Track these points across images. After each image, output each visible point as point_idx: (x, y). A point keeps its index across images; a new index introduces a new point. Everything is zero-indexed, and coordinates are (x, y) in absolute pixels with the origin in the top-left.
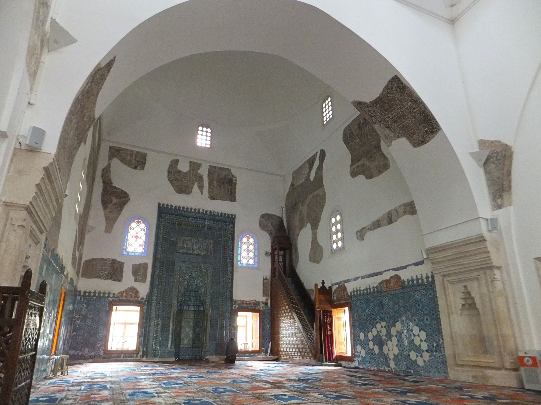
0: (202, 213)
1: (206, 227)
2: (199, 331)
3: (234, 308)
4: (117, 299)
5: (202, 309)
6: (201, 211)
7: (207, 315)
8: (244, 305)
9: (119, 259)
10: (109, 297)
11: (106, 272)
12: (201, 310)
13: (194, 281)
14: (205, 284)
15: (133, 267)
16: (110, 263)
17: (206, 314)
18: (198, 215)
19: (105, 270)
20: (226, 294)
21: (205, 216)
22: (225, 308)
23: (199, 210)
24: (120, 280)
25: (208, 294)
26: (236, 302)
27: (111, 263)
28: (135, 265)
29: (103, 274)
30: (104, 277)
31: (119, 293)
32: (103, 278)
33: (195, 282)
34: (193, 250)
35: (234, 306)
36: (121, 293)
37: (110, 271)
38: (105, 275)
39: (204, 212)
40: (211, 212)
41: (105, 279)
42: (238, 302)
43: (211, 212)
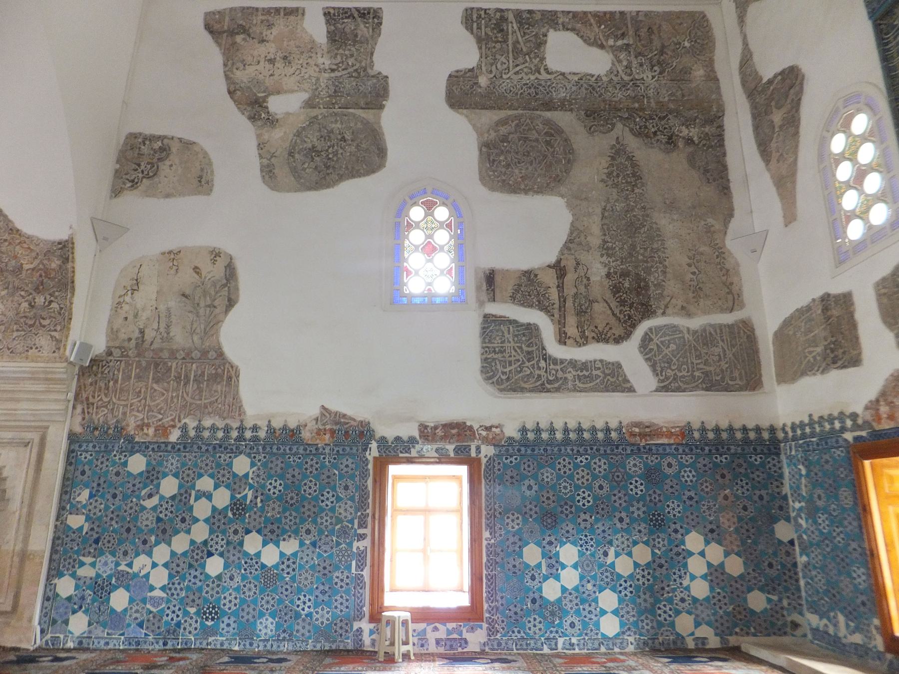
4: (864, 434)
9: (836, 288)
10: (843, 429)
11: (817, 346)
15: (879, 296)
16: (819, 312)
19: (814, 342)
24: (855, 361)
27: (823, 310)
28: (884, 279)
29: (814, 357)
30: (819, 367)
31: (867, 408)
32: (818, 370)
36: (873, 406)
37: (825, 339)
38: (818, 358)
41: (823, 372)
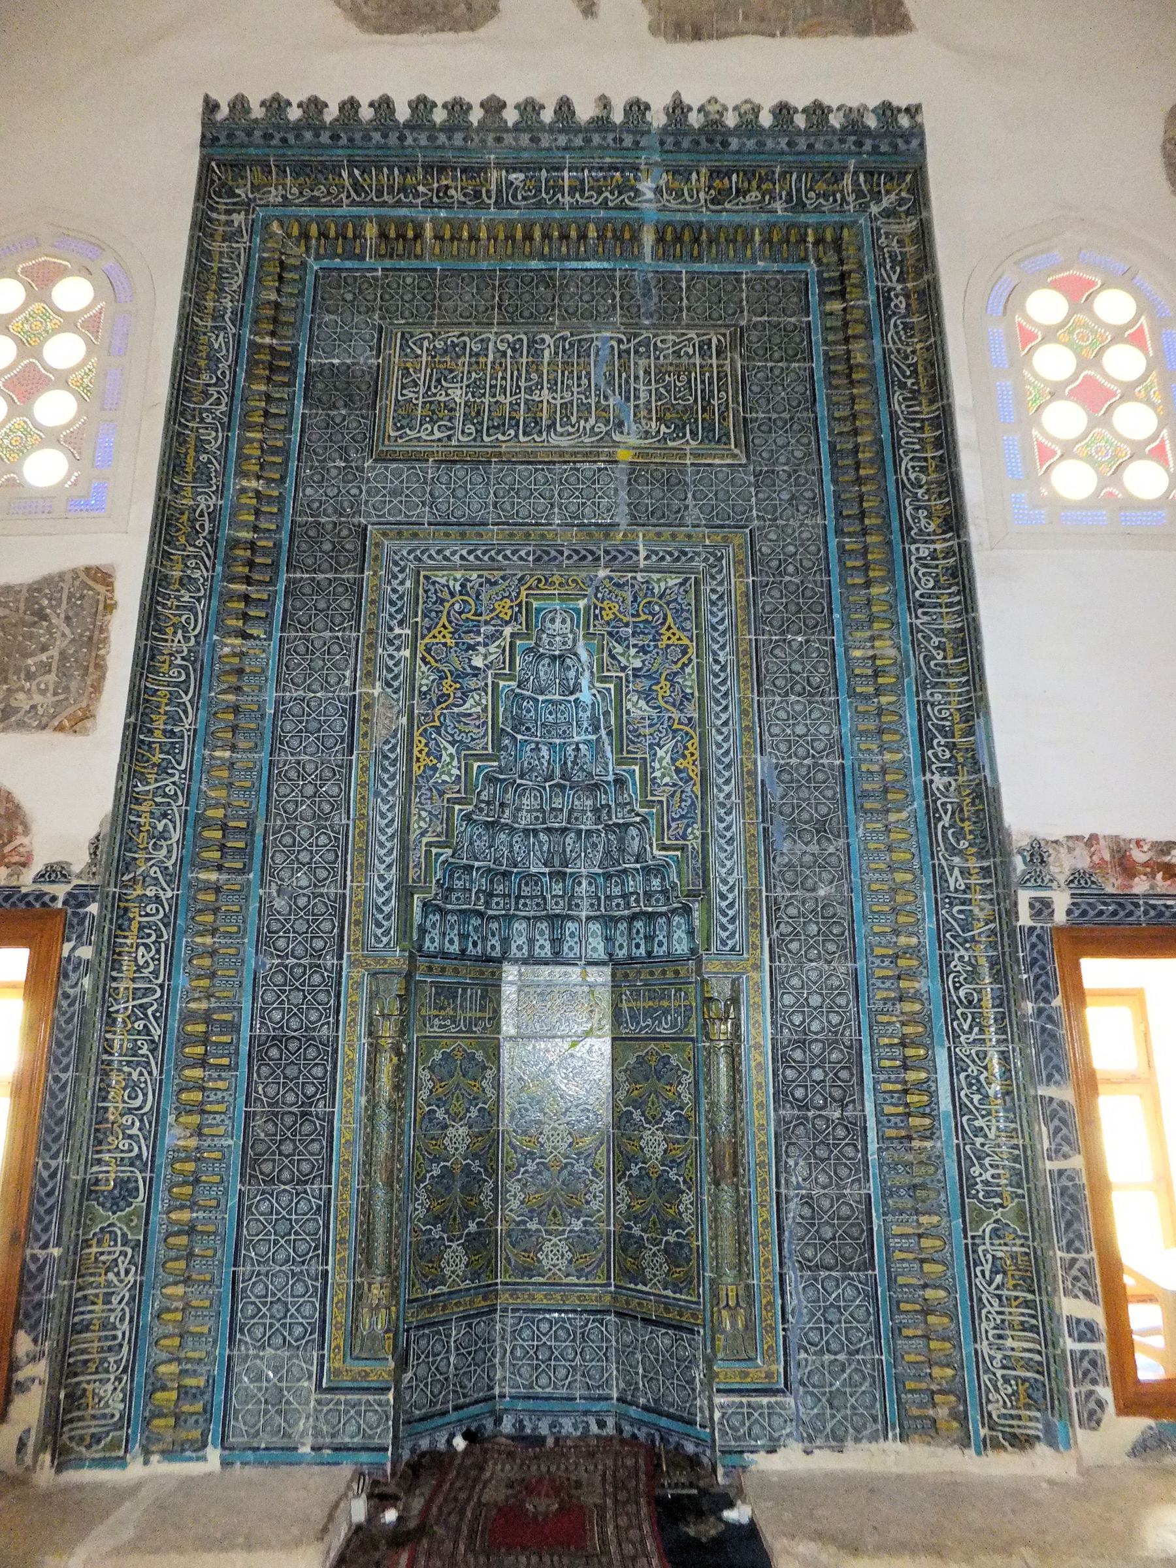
0: (601, 124)
1: (648, 238)
2: (669, 1161)
3: (1025, 918)
5: (681, 947)
6: (585, 112)
7: (735, 1000)
8: (1140, 886)
12: (672, 960)
13: (576, 688)
14: (681, 708)
17: (720, 989)
18: (562, 140)
20: (917, 781)
21: (628, 141)
22: (930, 924)
23: (565, 106)
25: (725, 790)
26: (1037, 854)
33: (585, 696)
34: (534, 424)
35: (1024, 897)
39: (618, 117)
40: (678, 109)
42: (1062, 866)
43: (678, 109)
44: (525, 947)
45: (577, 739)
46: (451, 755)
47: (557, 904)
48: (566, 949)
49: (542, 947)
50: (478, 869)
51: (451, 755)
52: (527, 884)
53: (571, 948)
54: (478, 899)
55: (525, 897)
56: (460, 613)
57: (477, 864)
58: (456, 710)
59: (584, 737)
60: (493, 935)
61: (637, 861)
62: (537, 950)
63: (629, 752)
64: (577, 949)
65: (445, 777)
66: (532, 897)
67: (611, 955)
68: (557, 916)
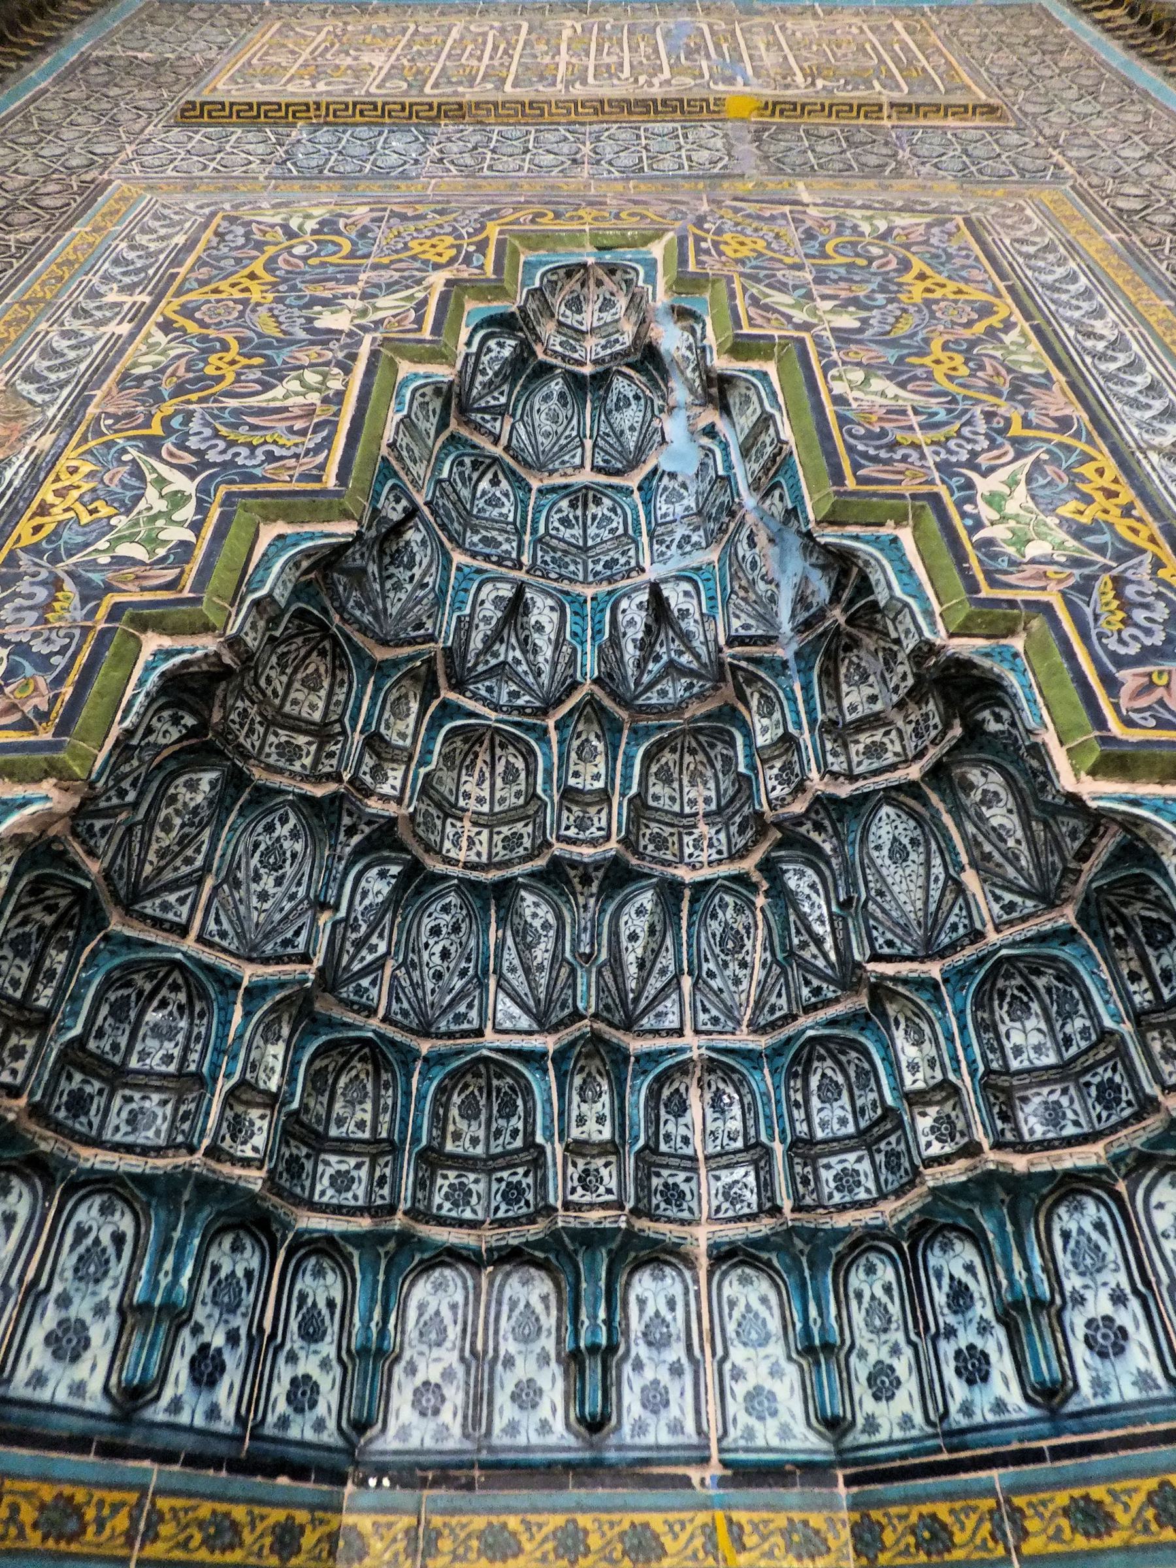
44: (455, 1396)
45: (653, 573)
46: (177, 500)
47: (587, 1180)
48: (631, 1400)
49: (527, 1395)
50: (256, 993)
51: (177, 500)
52: (470, 1112)
53: (655, 1400)
54: (238, 1128)
55: (464, 1163)
56: (305, 258)
57: (249, 973)
58: (233, 403)
59: (676, 562)
60: (312, 1333)
61: (930, 951)
62: (505, 1410)
63: (861, 481)
64: (681, 1406)
65: (138, 552)
66: (487, 1165)
67: (834, 1425)
68: (590, 1238)
